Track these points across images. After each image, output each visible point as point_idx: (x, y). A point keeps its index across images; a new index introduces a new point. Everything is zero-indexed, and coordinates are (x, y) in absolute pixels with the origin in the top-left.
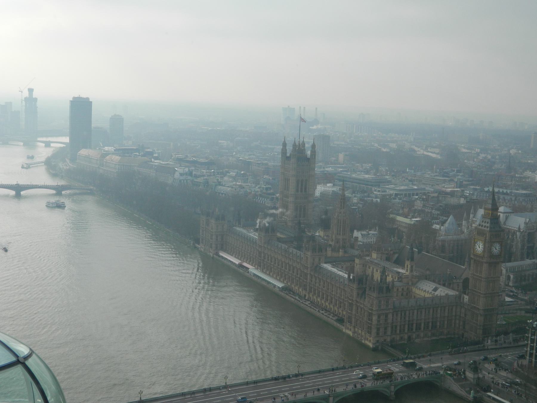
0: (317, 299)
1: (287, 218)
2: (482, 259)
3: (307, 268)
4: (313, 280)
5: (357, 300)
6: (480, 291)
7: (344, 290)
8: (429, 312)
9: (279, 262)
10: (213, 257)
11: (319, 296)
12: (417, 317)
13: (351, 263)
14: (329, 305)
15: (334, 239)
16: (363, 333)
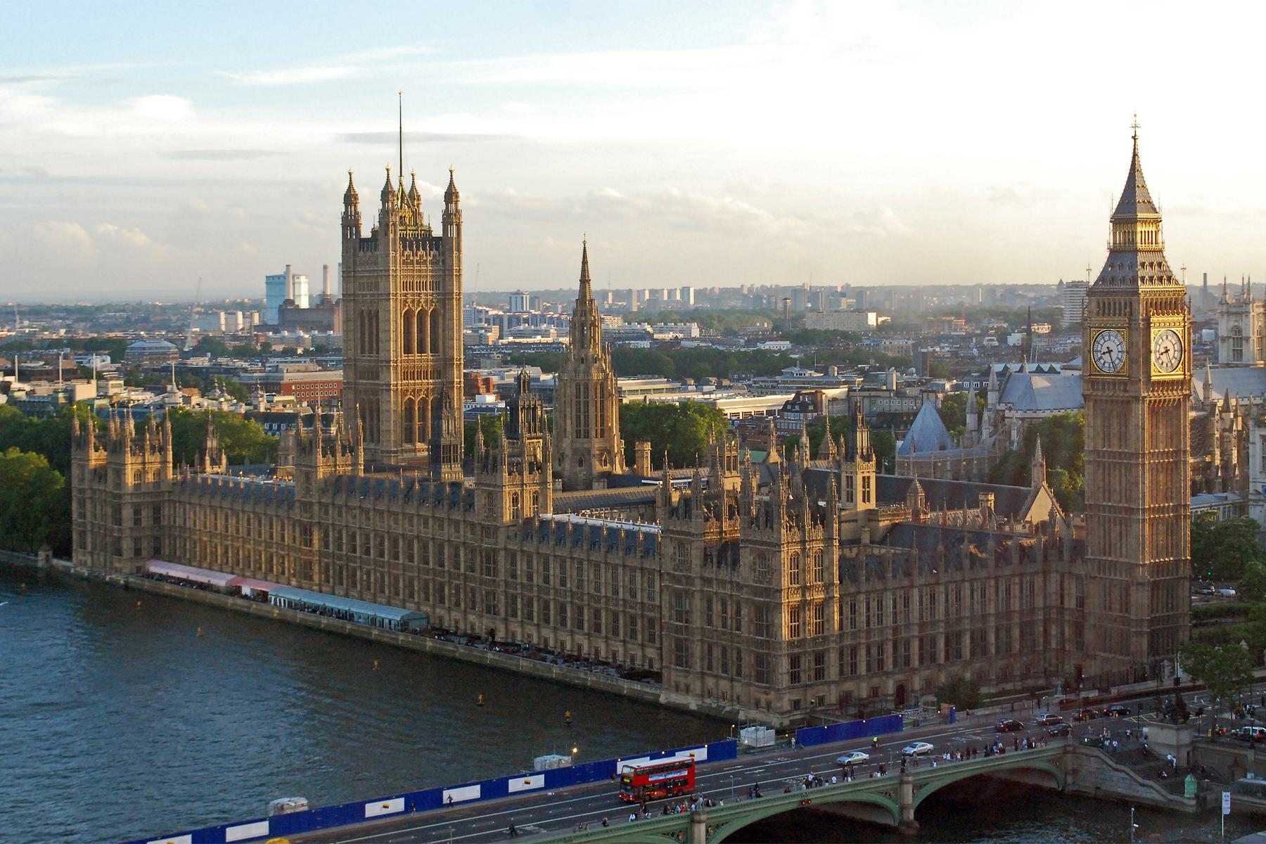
0: (539, 632)
1: (378, 447)
2: (1125, 391)
3: (490, 531)
4: (521, 567)
5: (706, 575)
6: (1126, 505)
7: (642, 569)
8: (958, 598)
9: (382, 544)
10: (126, 587)
11: (547, 621)
12: (921, 617)
13: (642, 510)
14: (590, 642)
15: (568, 452)
16: (738, 688)
